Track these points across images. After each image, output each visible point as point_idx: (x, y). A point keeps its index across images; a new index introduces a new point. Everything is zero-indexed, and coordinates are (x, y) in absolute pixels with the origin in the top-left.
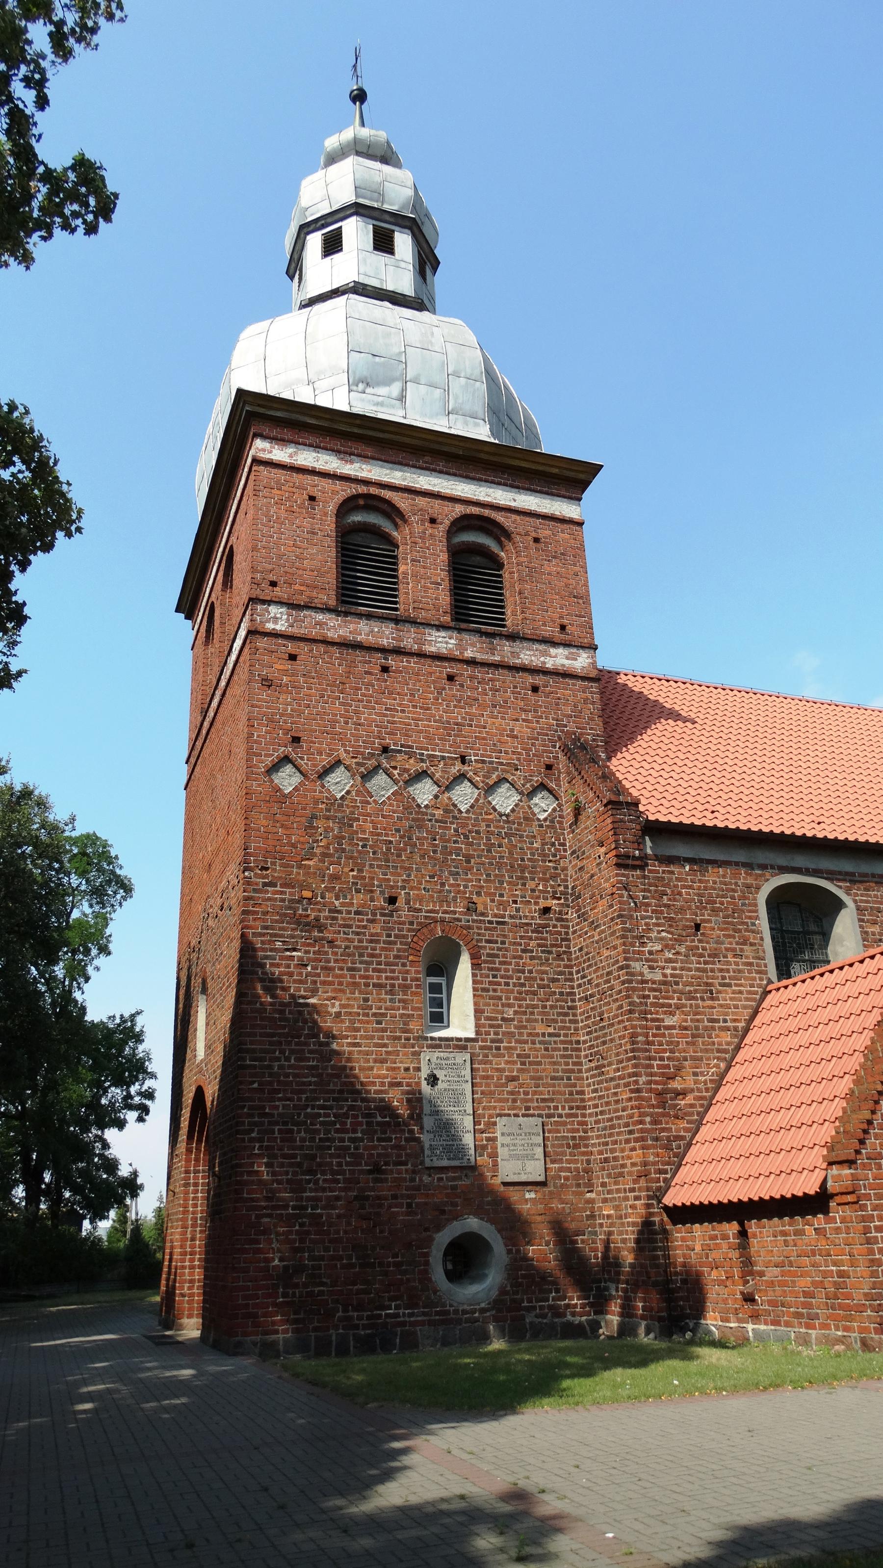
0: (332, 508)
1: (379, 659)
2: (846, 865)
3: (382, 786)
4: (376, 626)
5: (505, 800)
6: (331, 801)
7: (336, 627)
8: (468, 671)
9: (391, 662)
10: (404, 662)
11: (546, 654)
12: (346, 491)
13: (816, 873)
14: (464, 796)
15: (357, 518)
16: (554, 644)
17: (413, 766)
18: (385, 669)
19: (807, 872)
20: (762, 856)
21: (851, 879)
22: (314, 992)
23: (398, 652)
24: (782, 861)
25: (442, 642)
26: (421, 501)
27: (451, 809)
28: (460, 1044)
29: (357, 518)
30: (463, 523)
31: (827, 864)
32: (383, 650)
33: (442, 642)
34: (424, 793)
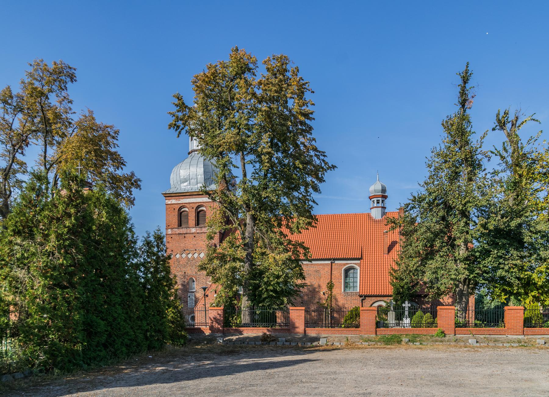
0: (177, 210)
1: (183, 235)
3: (184, 256)
5: (202, 255)
6: (177, 259)
7: (177, 231)
8: (197, 235)
12: (179, 206)
14: (196, 255)
15: (183, 210)
17: (188, 252)
23: (187, 233)
25: (193, 230)
26: (191, 205)
27: (194, 258)
29: (183, 210)
30: (199, 207)
33: (193, 230)
34: (190, 256)
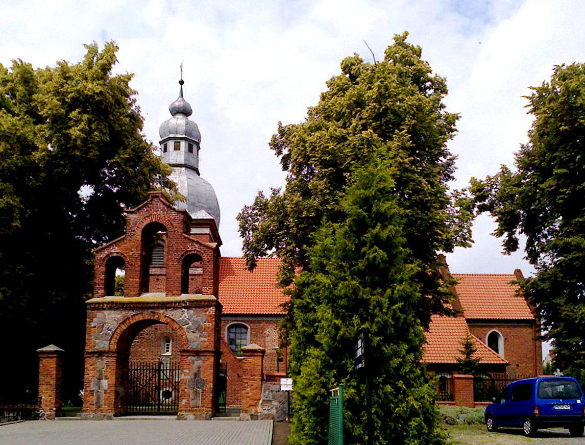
2: (250, 319)
4: (156, 269)
9: (159, 278)
10: (162, 277)
11: (196, 270)
13: (241, 321)
16: (198, 267)
18: (158, 279)
19: (240, 321)
20: (228, 318)
21: (251, 322)
22: (140, 348)
23: (161, 275)
24: (234, 319)
28: (168, 356)
31: (245, 319)
32: (158, 275)
